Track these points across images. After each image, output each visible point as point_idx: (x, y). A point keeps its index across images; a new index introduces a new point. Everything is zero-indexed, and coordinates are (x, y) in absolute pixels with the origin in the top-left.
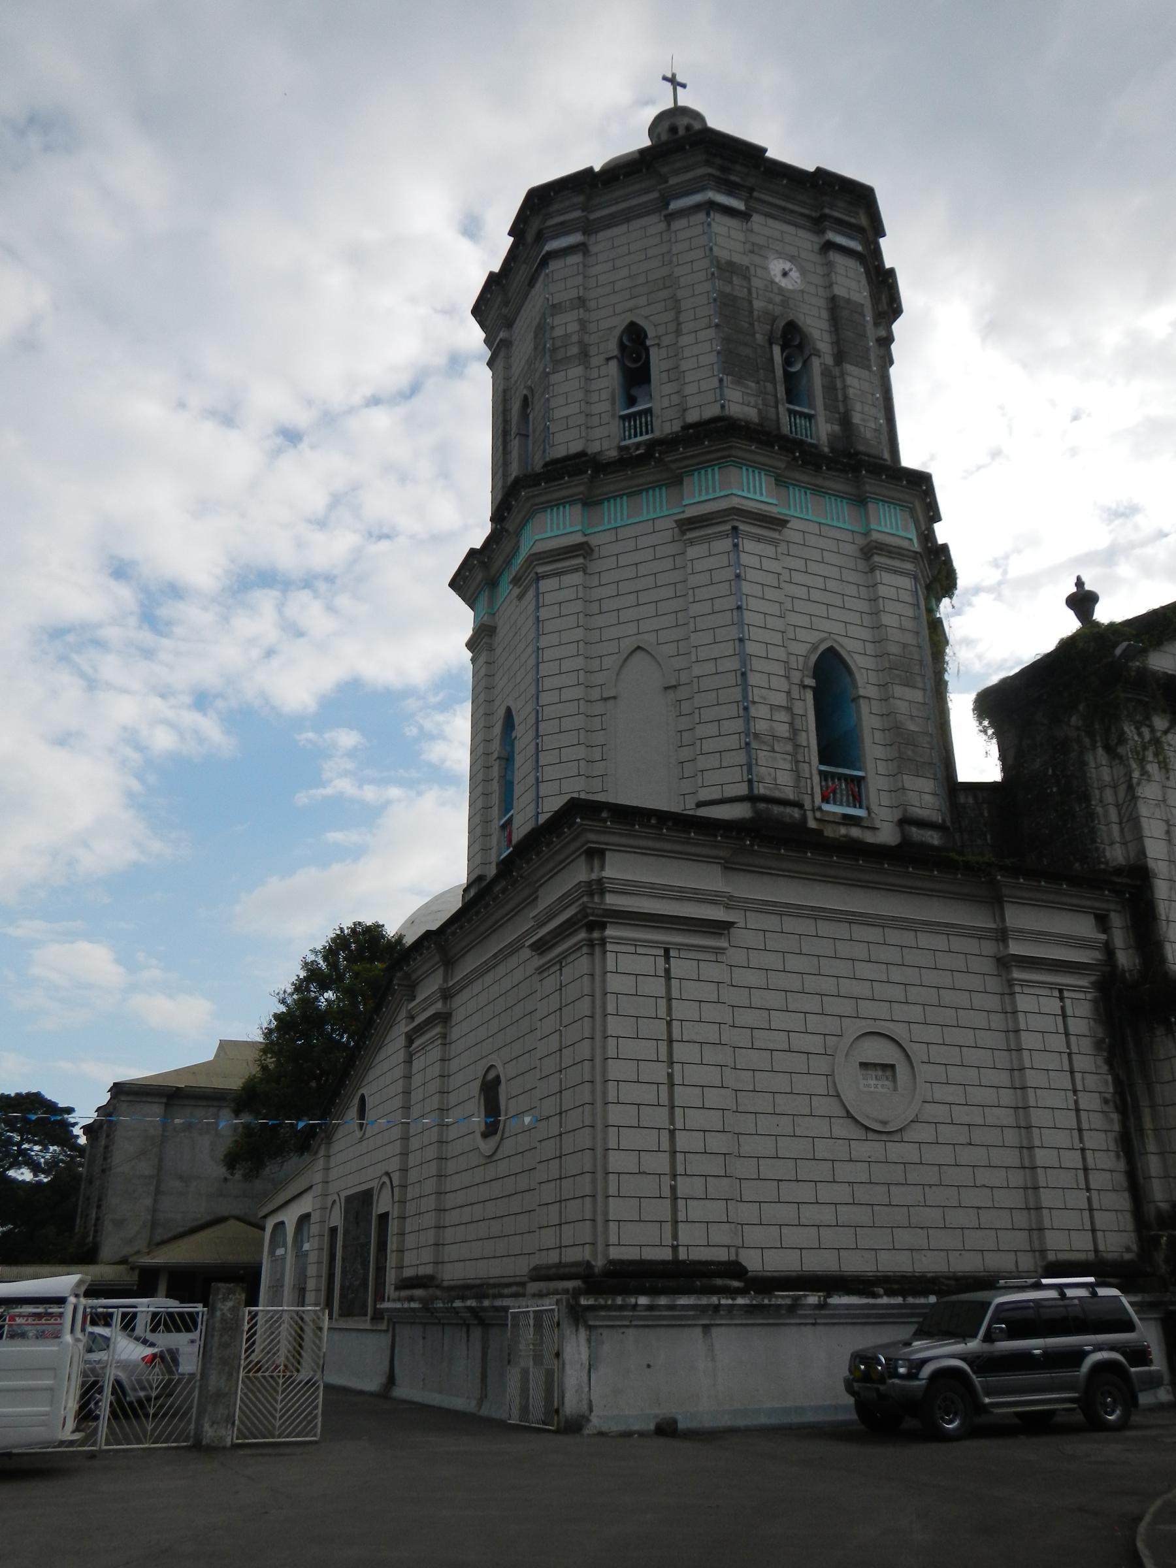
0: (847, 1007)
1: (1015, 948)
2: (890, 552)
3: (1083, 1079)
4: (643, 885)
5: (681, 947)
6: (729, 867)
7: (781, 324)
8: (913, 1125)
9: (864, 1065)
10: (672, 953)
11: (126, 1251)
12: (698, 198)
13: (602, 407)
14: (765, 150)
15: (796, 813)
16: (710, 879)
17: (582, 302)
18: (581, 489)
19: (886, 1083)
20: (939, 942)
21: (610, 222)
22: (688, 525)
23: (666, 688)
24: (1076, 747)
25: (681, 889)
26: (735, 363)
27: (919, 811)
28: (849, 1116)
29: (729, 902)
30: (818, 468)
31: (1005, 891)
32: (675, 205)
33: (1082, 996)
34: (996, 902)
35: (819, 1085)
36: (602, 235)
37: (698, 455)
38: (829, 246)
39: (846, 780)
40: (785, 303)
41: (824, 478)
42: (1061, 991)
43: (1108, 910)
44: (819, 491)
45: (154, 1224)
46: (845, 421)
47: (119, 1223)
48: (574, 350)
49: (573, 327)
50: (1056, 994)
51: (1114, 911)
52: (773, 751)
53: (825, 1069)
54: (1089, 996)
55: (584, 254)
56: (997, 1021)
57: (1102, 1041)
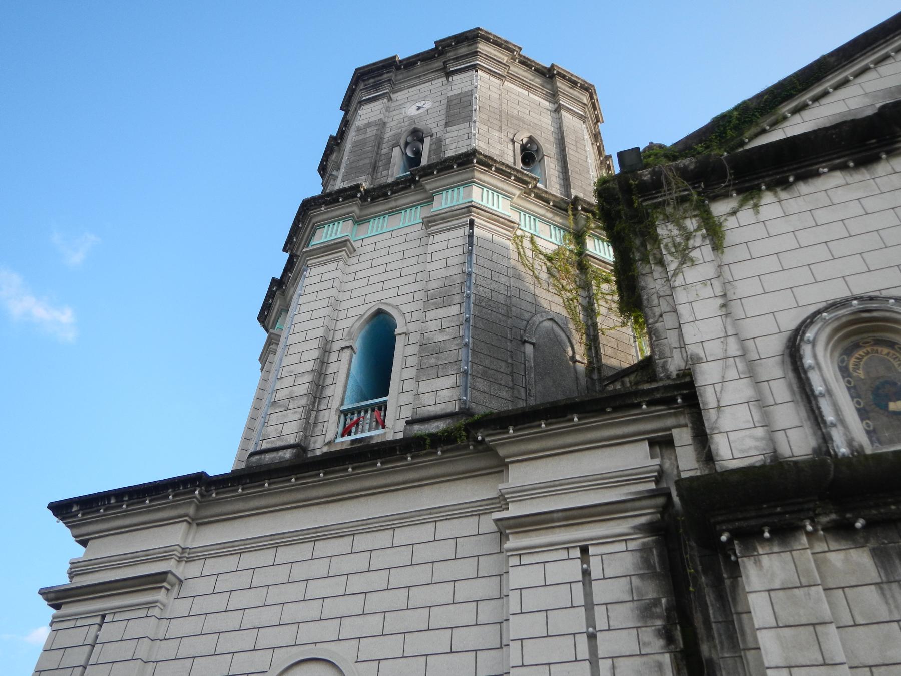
2: (444, 219)
3: (614, 667)
6: (197, 522)
30: (385, 196)
31: (502, 452)
33: (622, 547)
41: (395, 200)
42: (584, 550)
43: (669, 429)
50: (577, 553)
51: (675, 427)
54: (632, 545)
57: (656, 602)
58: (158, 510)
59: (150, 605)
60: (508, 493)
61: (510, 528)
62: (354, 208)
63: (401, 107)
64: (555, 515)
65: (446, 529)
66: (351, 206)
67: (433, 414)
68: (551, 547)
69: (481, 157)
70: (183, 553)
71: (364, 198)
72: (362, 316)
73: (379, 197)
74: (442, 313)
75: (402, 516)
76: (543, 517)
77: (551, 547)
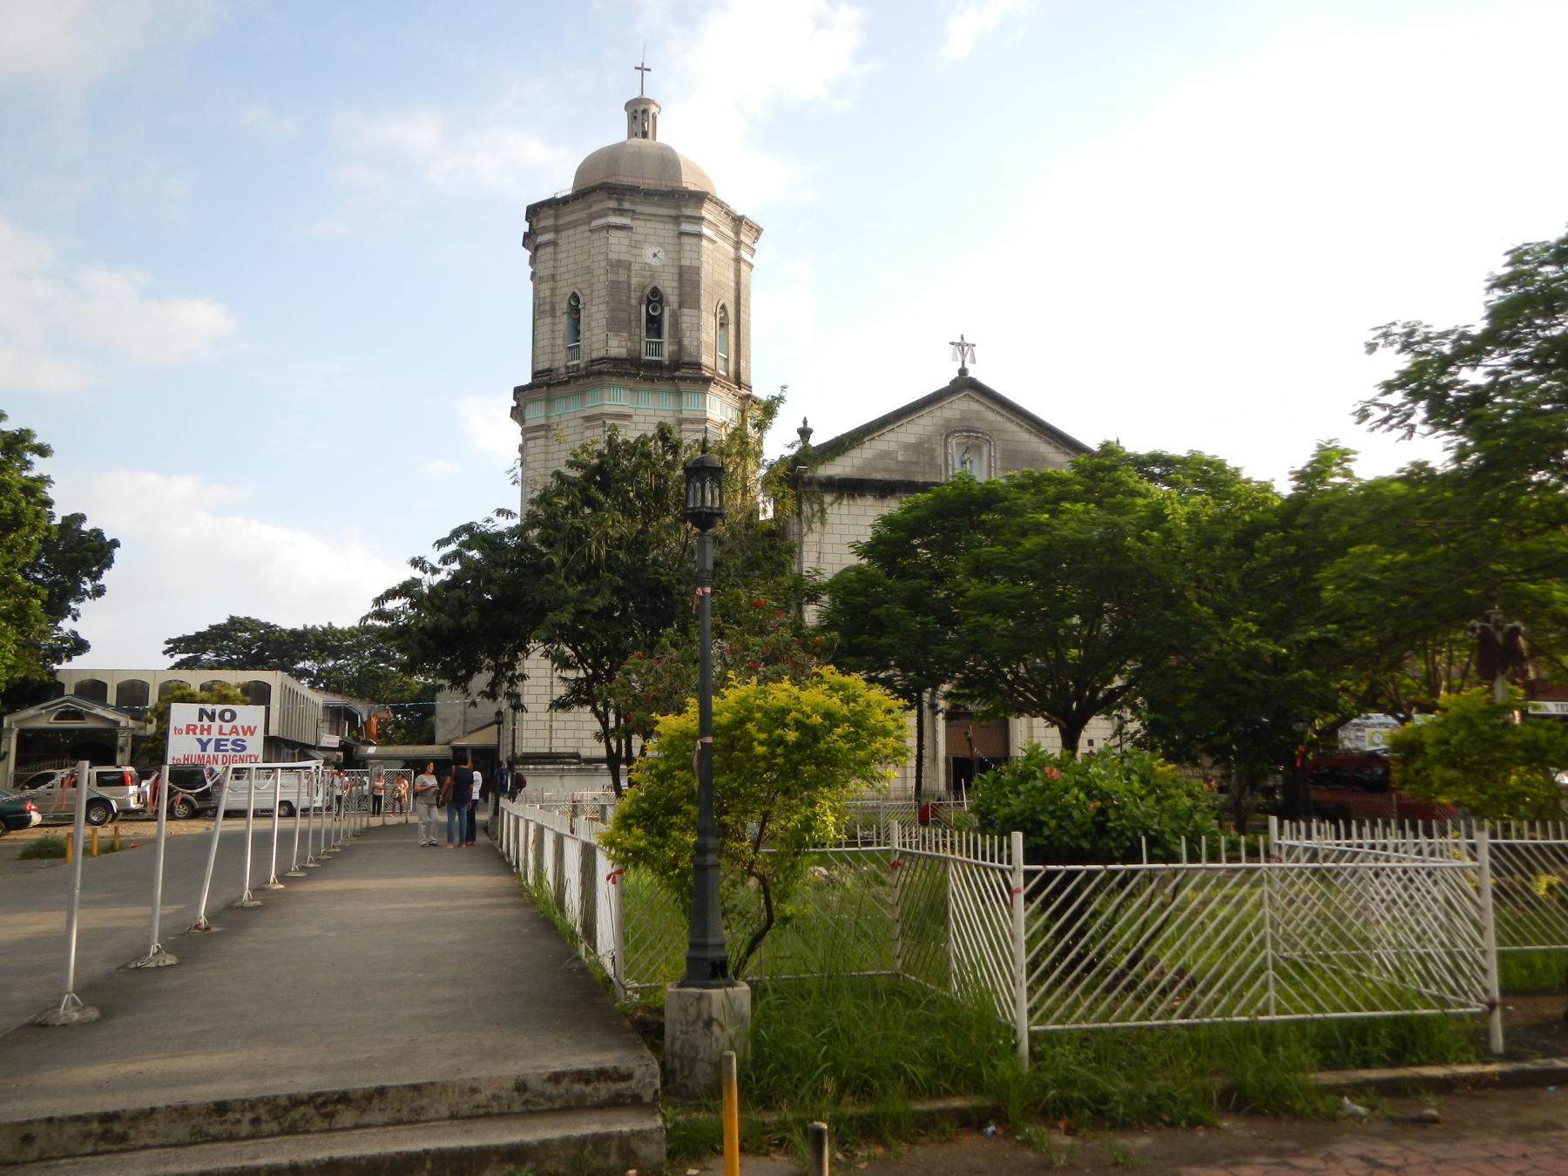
7: (648, 290)
11: (450, 737)
12: (603, 221)
13: (560, 341)
17: (553, 277)
21: (567, 226)
22: (588, 419)
26: (614, 324)
32: (595, 223)
36: (565, 234)
38: (682, 234)
40: (652, 277)
44: (656, 391)
45: (465, 721)
46: (680, 344)
47: (445, 721)
48: (547, 307)
49: (548, 293)
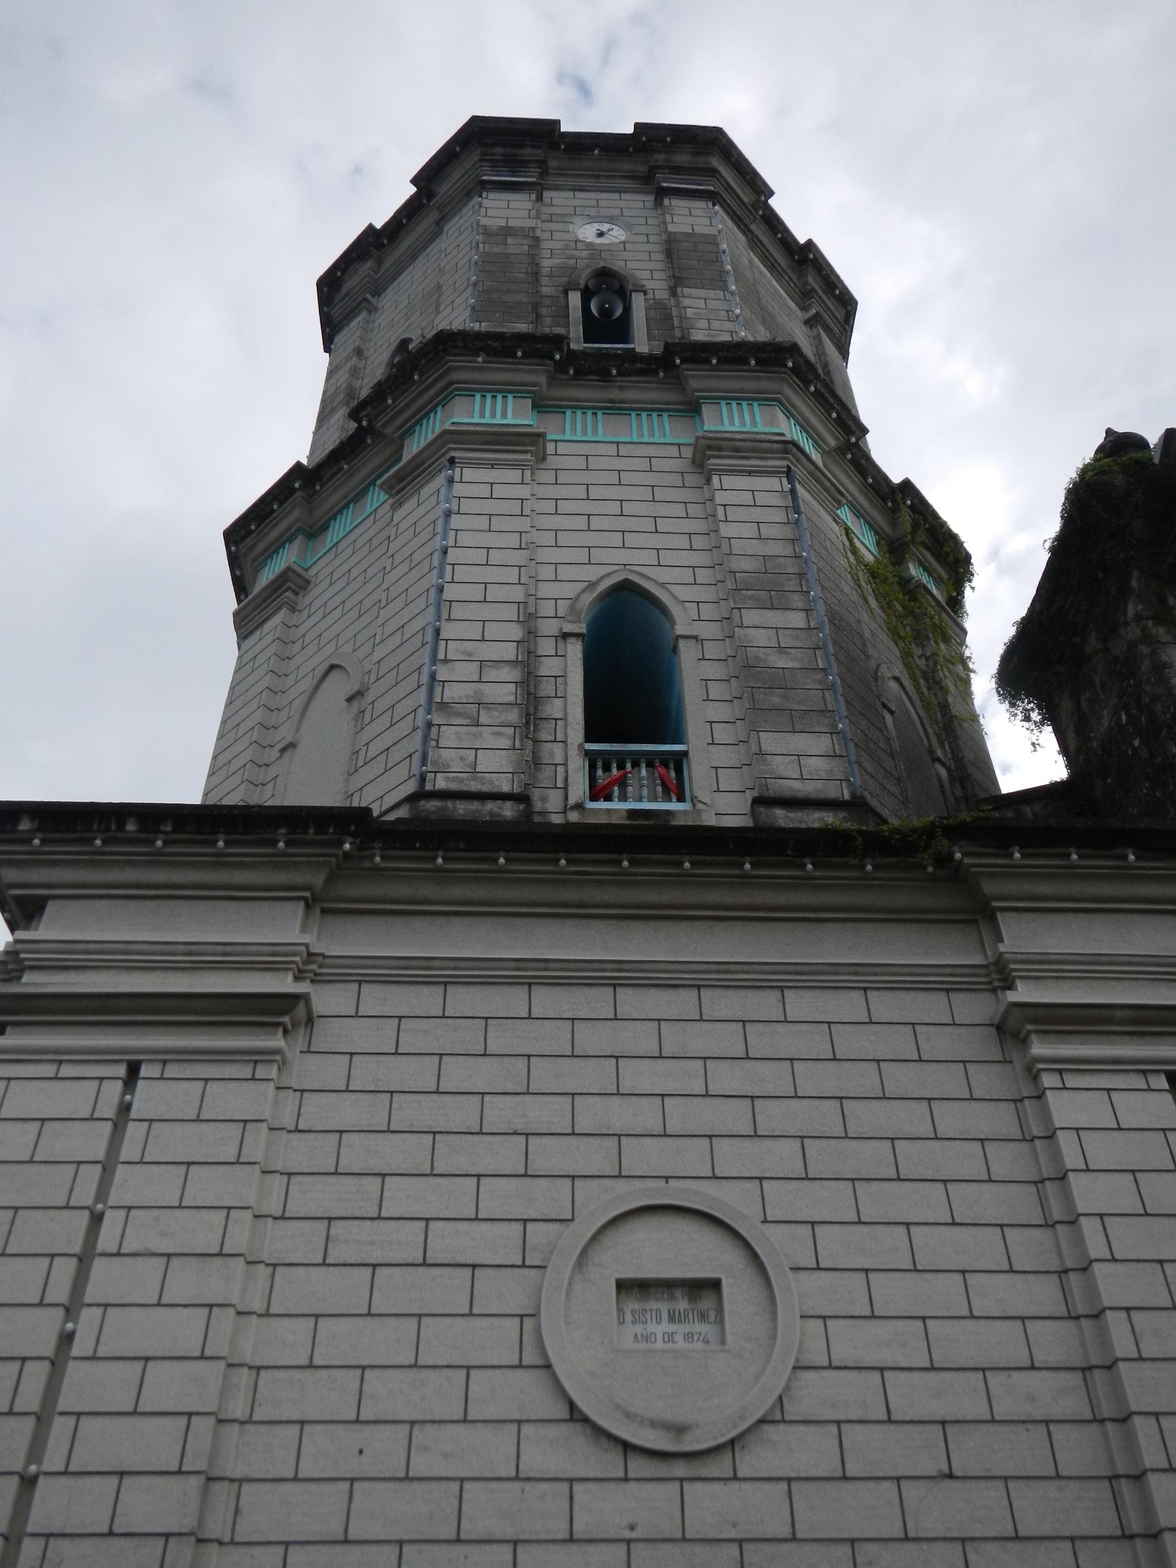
0: (597, 1156)
1: (1023, 993)
2: (737, 450)
4: (103, 947)
5: (165, 1057)
8: (768, 1429)
9: (623, 1286)
10: (144, 1071)
14: (557, 123)
15: (508, 811)
16: (283, 927)
18: (296, 513)
19: (703, 1328)
20: (847, 1006)
23: (349, 700)
24: (1145, 650)
25: (192, 947)
27: (797, 785)
28: (575, 1415)
29: (312, 966)
30: (605, 375)
31: (989, 888)
34: (980, 915)
35: (498, 1341)
37: (414, 400)
39: (650, 765)
41: (622, 388)
52: (478, 725)
53: (517, 1302)
55: (370, 312)
56: (1008, 1160)
58: (241, 866)
59: (256, 1057)
60: (1016, 962)
61: (1034, 1021)
62: (538, 376)
63: (563, 219)
64: (1119, 1013)
65: (887, 1005)
66: (535, 372)
67: (788, 794)
68: (1117, 1065)
69: (801, 360)
70: (306, 963)
71: (561, 367)
72: (592, 585)
73: (590, 372)
74: (774, 618)
75: (799, 969)
76: (1097, 1012)
77: (1117, 1065)
